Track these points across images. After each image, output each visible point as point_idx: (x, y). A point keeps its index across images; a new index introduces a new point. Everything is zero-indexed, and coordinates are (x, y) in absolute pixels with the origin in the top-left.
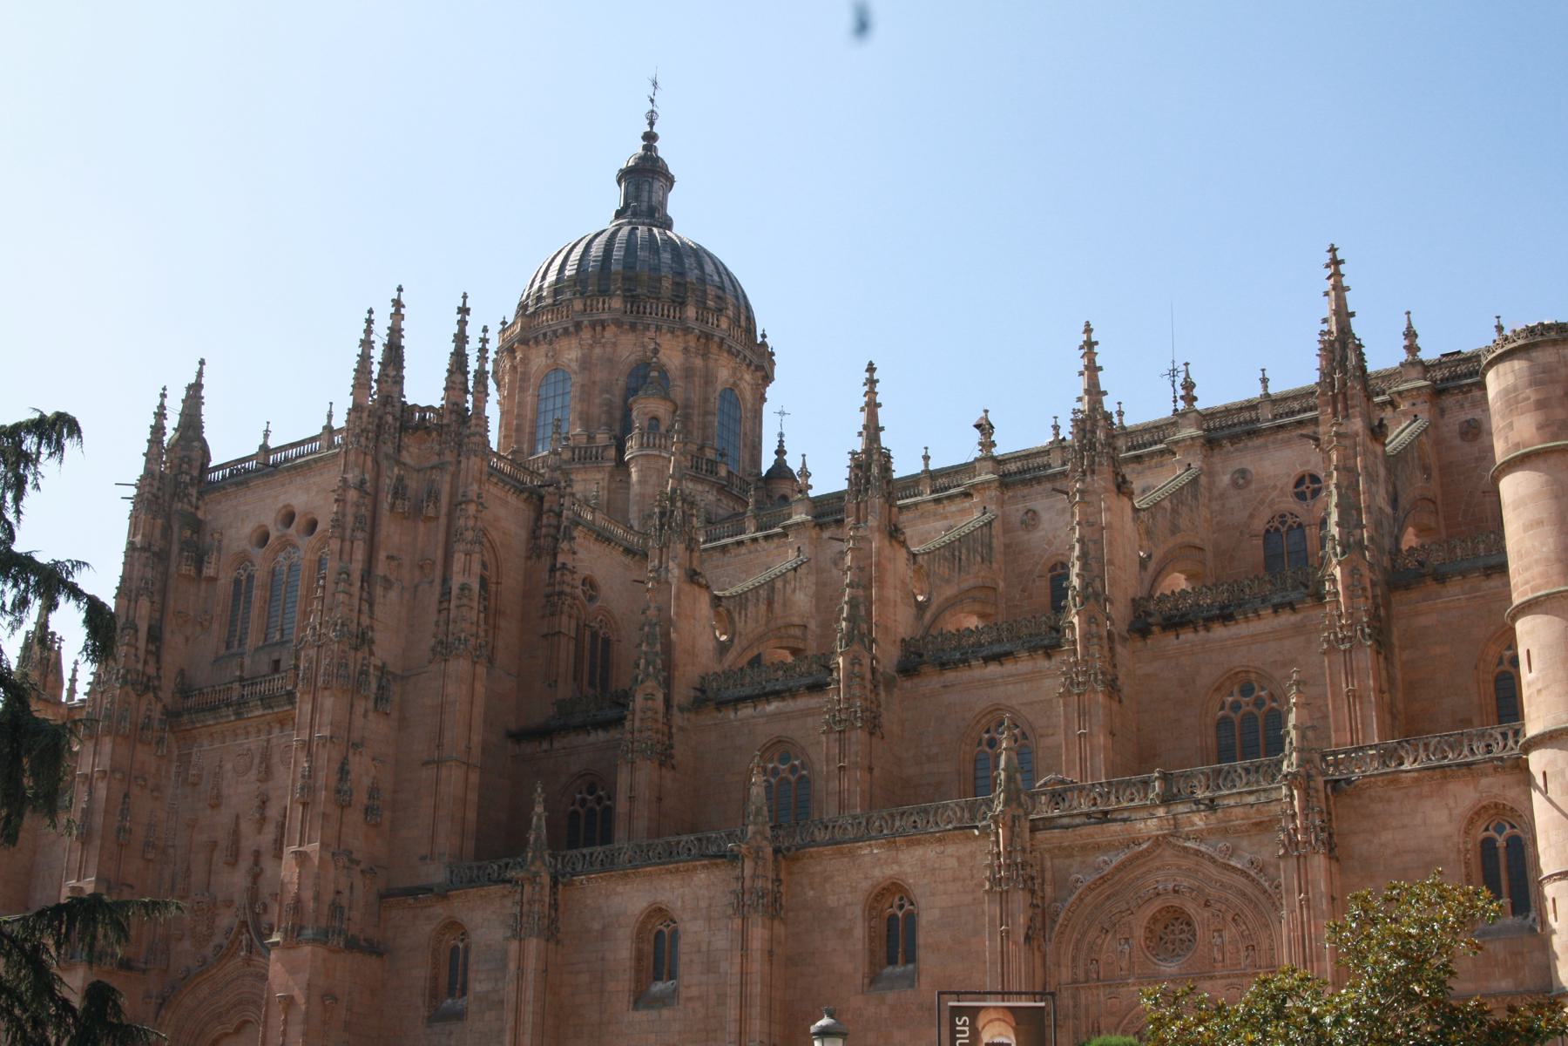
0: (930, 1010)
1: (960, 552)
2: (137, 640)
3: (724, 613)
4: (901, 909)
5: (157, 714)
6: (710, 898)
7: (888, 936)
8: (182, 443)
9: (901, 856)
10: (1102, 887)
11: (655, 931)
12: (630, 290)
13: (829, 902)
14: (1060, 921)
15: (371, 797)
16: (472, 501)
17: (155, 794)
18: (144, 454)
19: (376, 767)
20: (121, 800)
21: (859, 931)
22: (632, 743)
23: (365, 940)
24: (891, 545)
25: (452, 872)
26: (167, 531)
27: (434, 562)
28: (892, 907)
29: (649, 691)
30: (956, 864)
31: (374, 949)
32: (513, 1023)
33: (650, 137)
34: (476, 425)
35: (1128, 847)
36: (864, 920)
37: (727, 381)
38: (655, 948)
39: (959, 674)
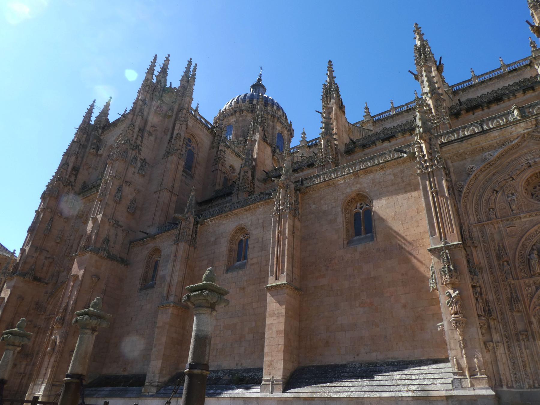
0: (384, 251)
3: (276, 159)
4: (361, 209)
6: (264, 218)
7: (355, 223)
8: (99, 117)
9: (361, 180)
10: (489, 169)
11: (239, 240)
12: (251, 104)
13: (323, 208)
14: (465, 190)
15: (131, 203)
16: (185, 109)
18: (84, 116)
19: (135, 193)
21: (340, 219)
22: (238, 188)
23: (119, 257)
24: (340, 112)
26: (87, 140)
28: (356, 208)
29: (246, 170)
30: (393, 178)
31: (124, 262)
33: (260, 80)
35: (503, 145)
36: (343, 213)
37: (280, 131)
38: (239, 247)
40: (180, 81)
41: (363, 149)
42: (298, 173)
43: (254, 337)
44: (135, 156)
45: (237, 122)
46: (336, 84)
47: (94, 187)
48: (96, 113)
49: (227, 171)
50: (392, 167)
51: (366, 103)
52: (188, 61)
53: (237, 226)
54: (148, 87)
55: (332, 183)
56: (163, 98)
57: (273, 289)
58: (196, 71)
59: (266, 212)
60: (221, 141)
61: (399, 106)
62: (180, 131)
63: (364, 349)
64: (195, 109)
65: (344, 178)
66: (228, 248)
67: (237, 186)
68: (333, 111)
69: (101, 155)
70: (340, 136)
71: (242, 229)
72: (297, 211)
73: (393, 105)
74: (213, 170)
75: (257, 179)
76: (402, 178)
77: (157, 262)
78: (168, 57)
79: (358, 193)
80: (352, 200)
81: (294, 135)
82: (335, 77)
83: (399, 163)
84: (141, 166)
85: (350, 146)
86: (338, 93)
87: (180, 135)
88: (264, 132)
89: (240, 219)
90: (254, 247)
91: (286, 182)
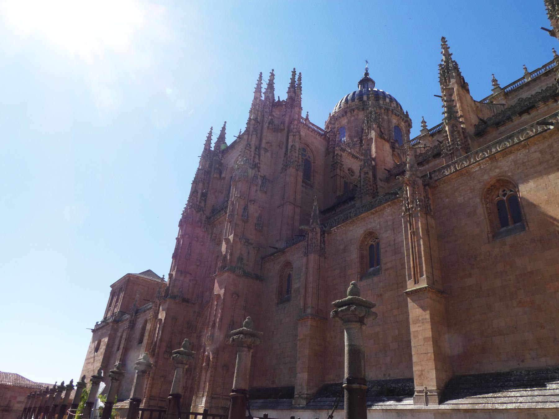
1: (493, 109)
2: (197, 195)
3: (397, 155)
5: (204, 218)
6: (393, 219)
9: (500, 164)
12: (361, 101)
13: (459, 201)
16: (296, 120)
17: (202, 244)
18: (204, 144)
19: (260, 210)
20: (188, 245)
21: (481, 210)
22: (360, 191)
23: (254, 274)
24: (463, 91)
25: (287, 243)
27: (283, 143)
28: (498, 196)
29: (366, 171)
30: (540, 155)
31: (258, 278)
32: (304, 294)
33: (367, 74)
34: (297, 99)
36: (483, 204)
37: (396, 123)
39: (506, 126)
40: (287, 93)
41: (497, 127)
42: (423, 166)
43: (399, 346)
44: (255, 174)
45: (349, 122)
46: (454, 61)
47: (222, 209)
48: (214, 139)
49: (347, 175)
50: (537, 143)
51: (493, 75)
52: (292, 72)
53: (365, 231)
54: (258, 105)
55: (465, 171)
56: (273, 113)
57: (414, 293)
58: (301, 80)
59: (394, 213)
60: (336, 145)
61: (536, 70)
62: (294, 142)
63: (530, 354)
64: (305, 117)
65: (479, 165)
66: (359, 255)
67: (359, 189)
68: (454, 92)
69: (224, 178)
70: (466, 118)
71: (370, 234)
72: (429, 208)
73: (526, 70)
74: (332, 176)
75: (379, 178)
76: (551, 154)
77: (289, 276)
78: (273, 72)
79: (498, 178)
80: (493, 187)
81: (413, 125)
82: (451, 54)
83: (545, 138)
84: (262, 183)
85: (481, 127)
86: (458, 71)
87: (295, 147)
88: (380, 128)
89: (367, 223)
90: (386, 251)
91: (412, 178)
